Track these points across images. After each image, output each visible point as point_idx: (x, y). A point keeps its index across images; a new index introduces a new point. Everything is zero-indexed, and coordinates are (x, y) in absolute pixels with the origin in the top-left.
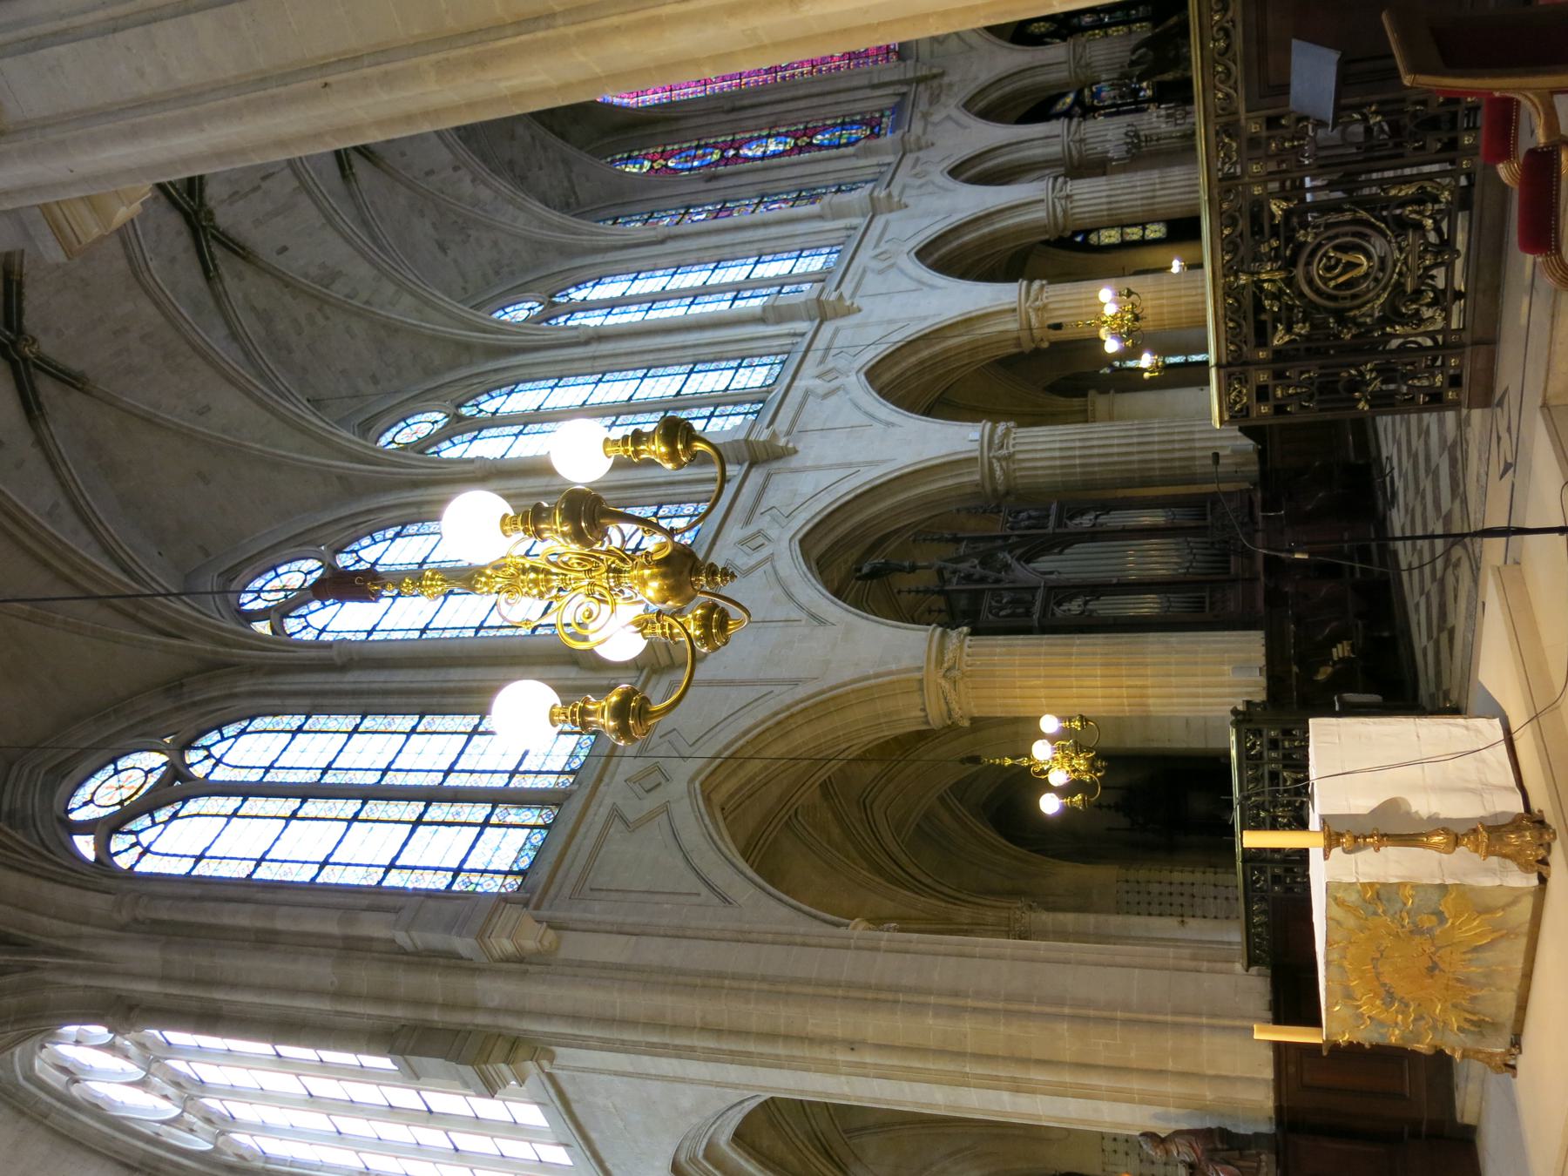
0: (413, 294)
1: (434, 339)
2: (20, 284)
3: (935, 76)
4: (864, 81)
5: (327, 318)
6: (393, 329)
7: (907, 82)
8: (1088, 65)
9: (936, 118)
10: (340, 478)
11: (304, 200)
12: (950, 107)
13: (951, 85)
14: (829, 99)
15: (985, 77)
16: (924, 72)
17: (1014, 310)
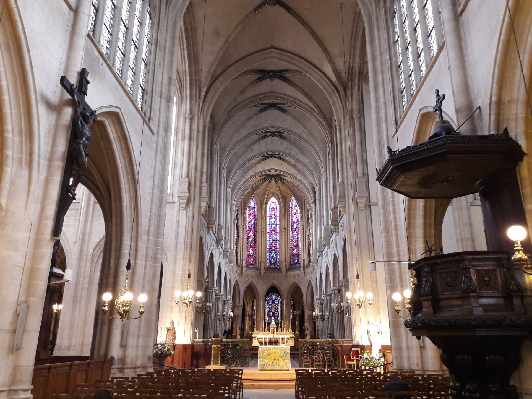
0: (243, 164)
1: (233, 167)
2: (283, 112)
3: (242, 274)
4: (244, 258)
5: (244, 146)
6: (238, 158)
7: (242, 268)
8: (238, 308)
9: (236, 274)
10: (225, 148)
11: (266, 150)
12: (237, 278)
13: (240, 277)
14: (242, 249)
15: (240, 285)
16: (244, 271)
17: (221, 293)
